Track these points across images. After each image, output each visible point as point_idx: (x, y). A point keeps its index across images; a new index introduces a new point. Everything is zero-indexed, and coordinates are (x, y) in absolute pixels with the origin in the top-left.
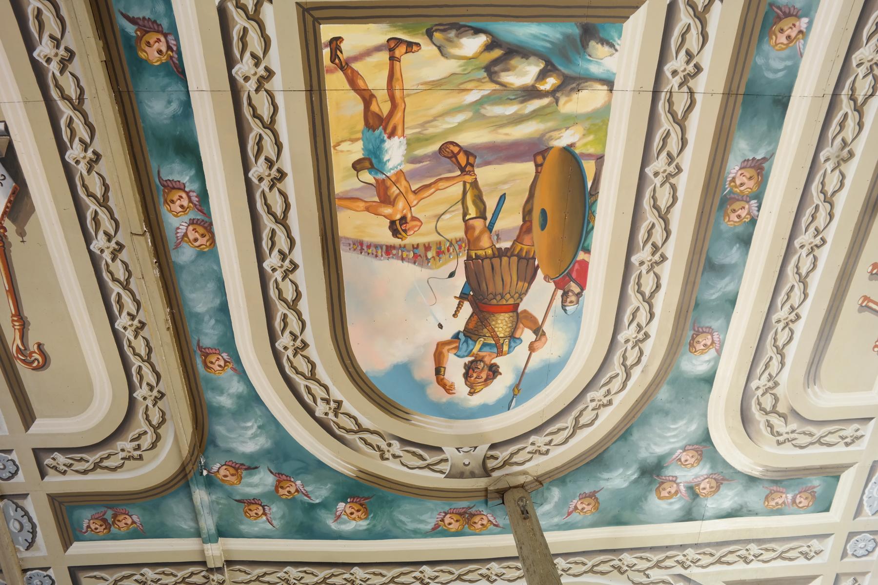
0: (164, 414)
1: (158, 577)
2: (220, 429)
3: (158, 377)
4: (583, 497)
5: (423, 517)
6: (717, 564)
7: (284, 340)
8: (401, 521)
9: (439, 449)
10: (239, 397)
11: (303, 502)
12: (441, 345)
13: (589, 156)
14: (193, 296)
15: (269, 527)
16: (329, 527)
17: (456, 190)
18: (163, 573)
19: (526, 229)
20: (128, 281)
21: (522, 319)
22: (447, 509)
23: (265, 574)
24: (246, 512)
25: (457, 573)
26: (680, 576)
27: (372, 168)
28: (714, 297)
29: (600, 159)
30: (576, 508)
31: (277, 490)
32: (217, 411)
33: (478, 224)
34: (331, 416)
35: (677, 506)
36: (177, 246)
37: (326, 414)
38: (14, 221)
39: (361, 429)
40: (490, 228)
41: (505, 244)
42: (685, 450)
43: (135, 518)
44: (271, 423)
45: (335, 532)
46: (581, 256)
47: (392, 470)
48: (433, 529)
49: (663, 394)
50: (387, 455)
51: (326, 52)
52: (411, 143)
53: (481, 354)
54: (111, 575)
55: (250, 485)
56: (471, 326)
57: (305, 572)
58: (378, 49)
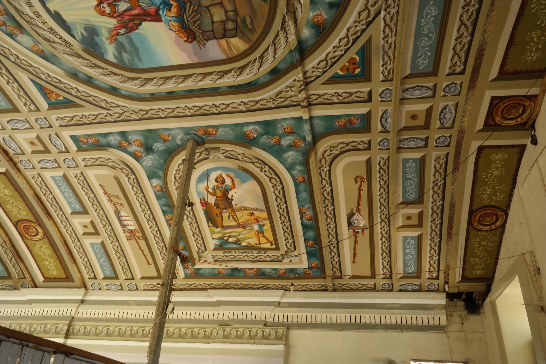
0: (320, 162)
1: (331, 98)
2: (301, 158)
3: (320, 174)
4: (168, 141)
5: (223, 133)
7: (279, 188)
8: (231, 131)
9: (226, 157)
10: (294, 169)
11: (270, 135)
12: (234, 188)
13: (212, 227)
14: (306, 196)
15: (282, 124)
16: (259, 127)
17: (240, 221)
18: (329, 100)
19: (221, 213)
20: (325, 199)
21: (214, 194)
22: (216, 136)
23: (283, 102)
24: (292, 129)
25: (202, 110)
27: (261, 225)
28: (163, 200)
29: (209, 226)
30: (168, 136)
31: (280, 139)
32: (301, 164)
33: (233, 214)
34: (263, 167)
35: (130, 137)
36: (309, 208)
37: (265, 167)
38: (353, 213)
39: (253, 163)
40: (230, 214)
41: (224, 210)
42: (142, 156)
43: (337, 124)
44: (283, 162)
45: (256, 125)
46: (205, 208)
47: (239, 150)
48: (218, 129)
49: (161, 173)
50: (242, 155)
51: (273, 243)
52: (253, 229)
53: (222, 186)
54: (353, 98)
55: (290, 140)
56: (227, 193)
57: (266, 105)
58: (263, 244)
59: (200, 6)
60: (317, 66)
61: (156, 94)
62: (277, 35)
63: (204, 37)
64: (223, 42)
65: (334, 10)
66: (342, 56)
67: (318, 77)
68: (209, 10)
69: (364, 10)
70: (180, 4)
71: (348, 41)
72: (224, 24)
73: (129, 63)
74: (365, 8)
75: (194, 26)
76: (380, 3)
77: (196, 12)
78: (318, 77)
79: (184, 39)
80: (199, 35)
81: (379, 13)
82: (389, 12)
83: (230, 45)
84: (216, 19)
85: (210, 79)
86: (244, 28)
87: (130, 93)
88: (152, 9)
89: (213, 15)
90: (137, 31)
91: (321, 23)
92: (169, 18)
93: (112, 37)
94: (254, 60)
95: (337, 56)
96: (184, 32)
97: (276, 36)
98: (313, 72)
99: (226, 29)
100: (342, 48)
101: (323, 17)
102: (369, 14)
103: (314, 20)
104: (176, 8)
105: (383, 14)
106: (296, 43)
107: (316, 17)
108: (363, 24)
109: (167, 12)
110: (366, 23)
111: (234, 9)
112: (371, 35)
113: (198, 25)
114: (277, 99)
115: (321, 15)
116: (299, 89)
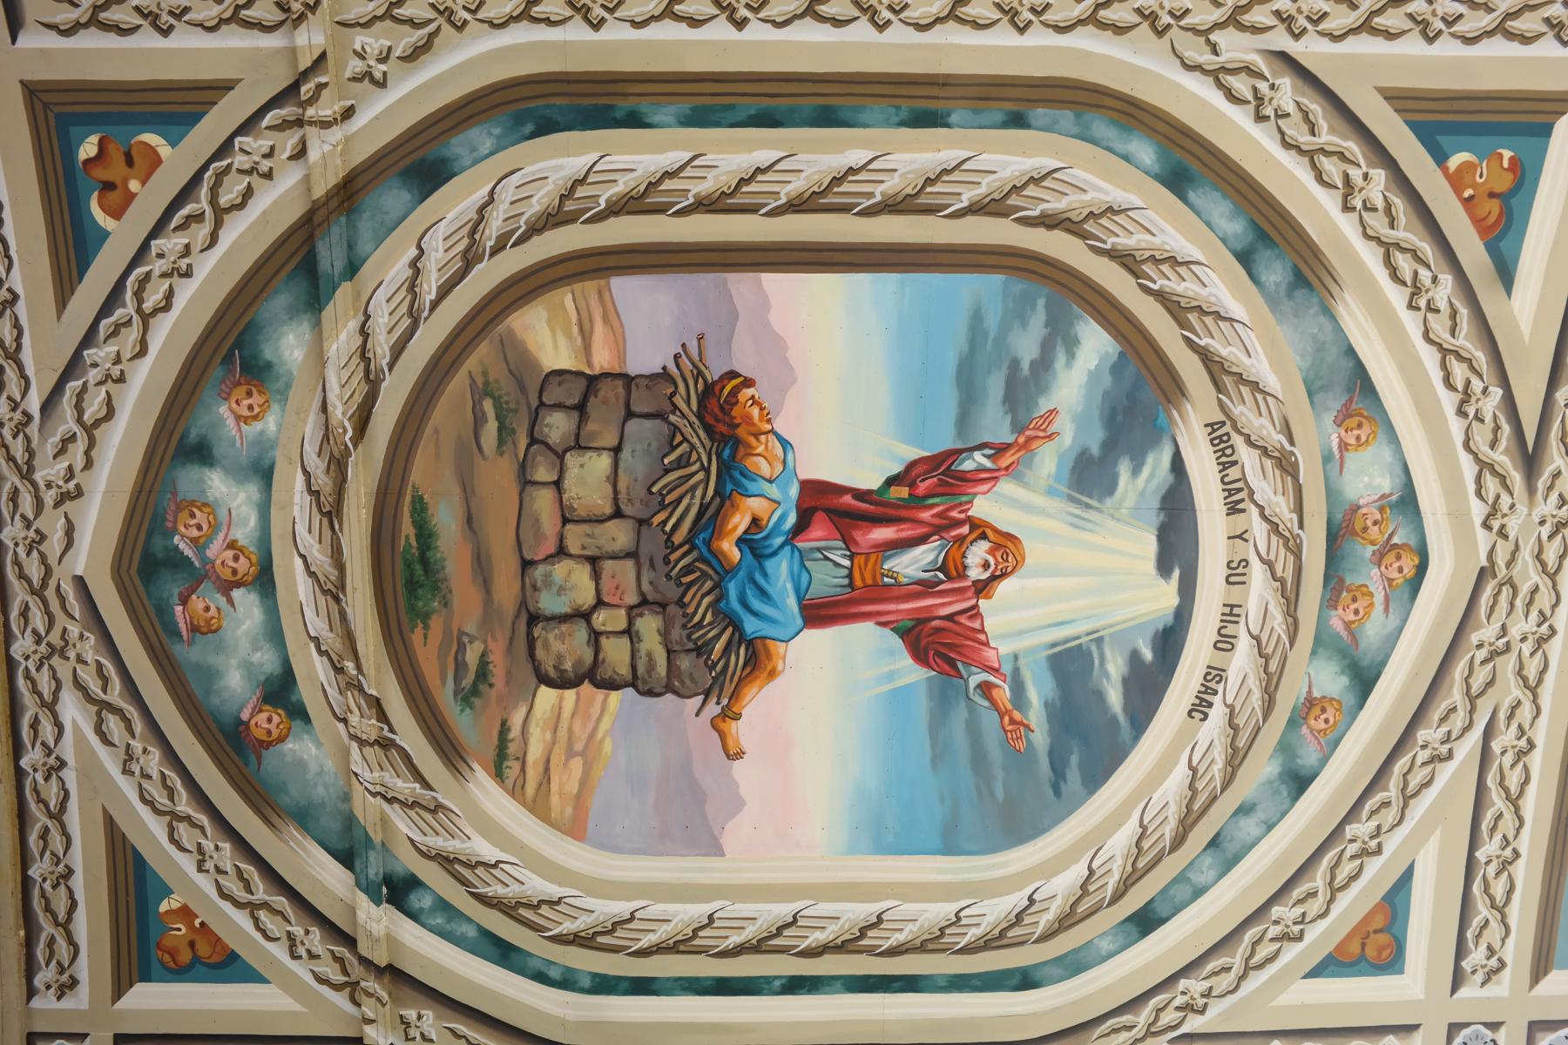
6: (1364, 35)
26: (1284, 57)
59: (642, 522)
60: (255, 180)
61: (999, 117)
62: (398, 351)
63: (672, 390)
64: (602, 360)
65: (193, 435)
66: (157, 231)
67: (248, 126)
68: (616, 500)
69: (98, 423)
70: (708, 543)
71: (139, 295)
72: (578, 436)
73: (1034, 309)
74: (95, 432)
75: (693, 447)
76: (49, 446)
77: (663, 500)
78: (246, 127)
79: (750, 392)
80: (687, 402)
81: (48, 406)
82: (14, 410)
83: (579, 340)
84: (603, 462)
85: (711, 174)
86: (512, 405)
87: (1119, 147)
88: (819, 531)
89: (608, 478)
90: (915, 453)
91: (239, 384)
92: (773, 491)
93: (1030, 439)
94: (504, 247)
95: (176, 229)
96: (738, 425)
97: (403, 347)
98: (270, 154)
99: (576, 414)
100: (159, 266)
101: (232, 411)
102: (79, 409)
103: (261, 400)
104: (730, 526)
105: (34, 403)
106: (328, 313)
107: (257, 410)
108: (95, 365)
109: (766, 519)
110: (84, 373)
111: (529, 488)
112: (59, 317)
113: (674, 448)
114: (431, 14)
115: (238, 418)
116: (323, 80)
